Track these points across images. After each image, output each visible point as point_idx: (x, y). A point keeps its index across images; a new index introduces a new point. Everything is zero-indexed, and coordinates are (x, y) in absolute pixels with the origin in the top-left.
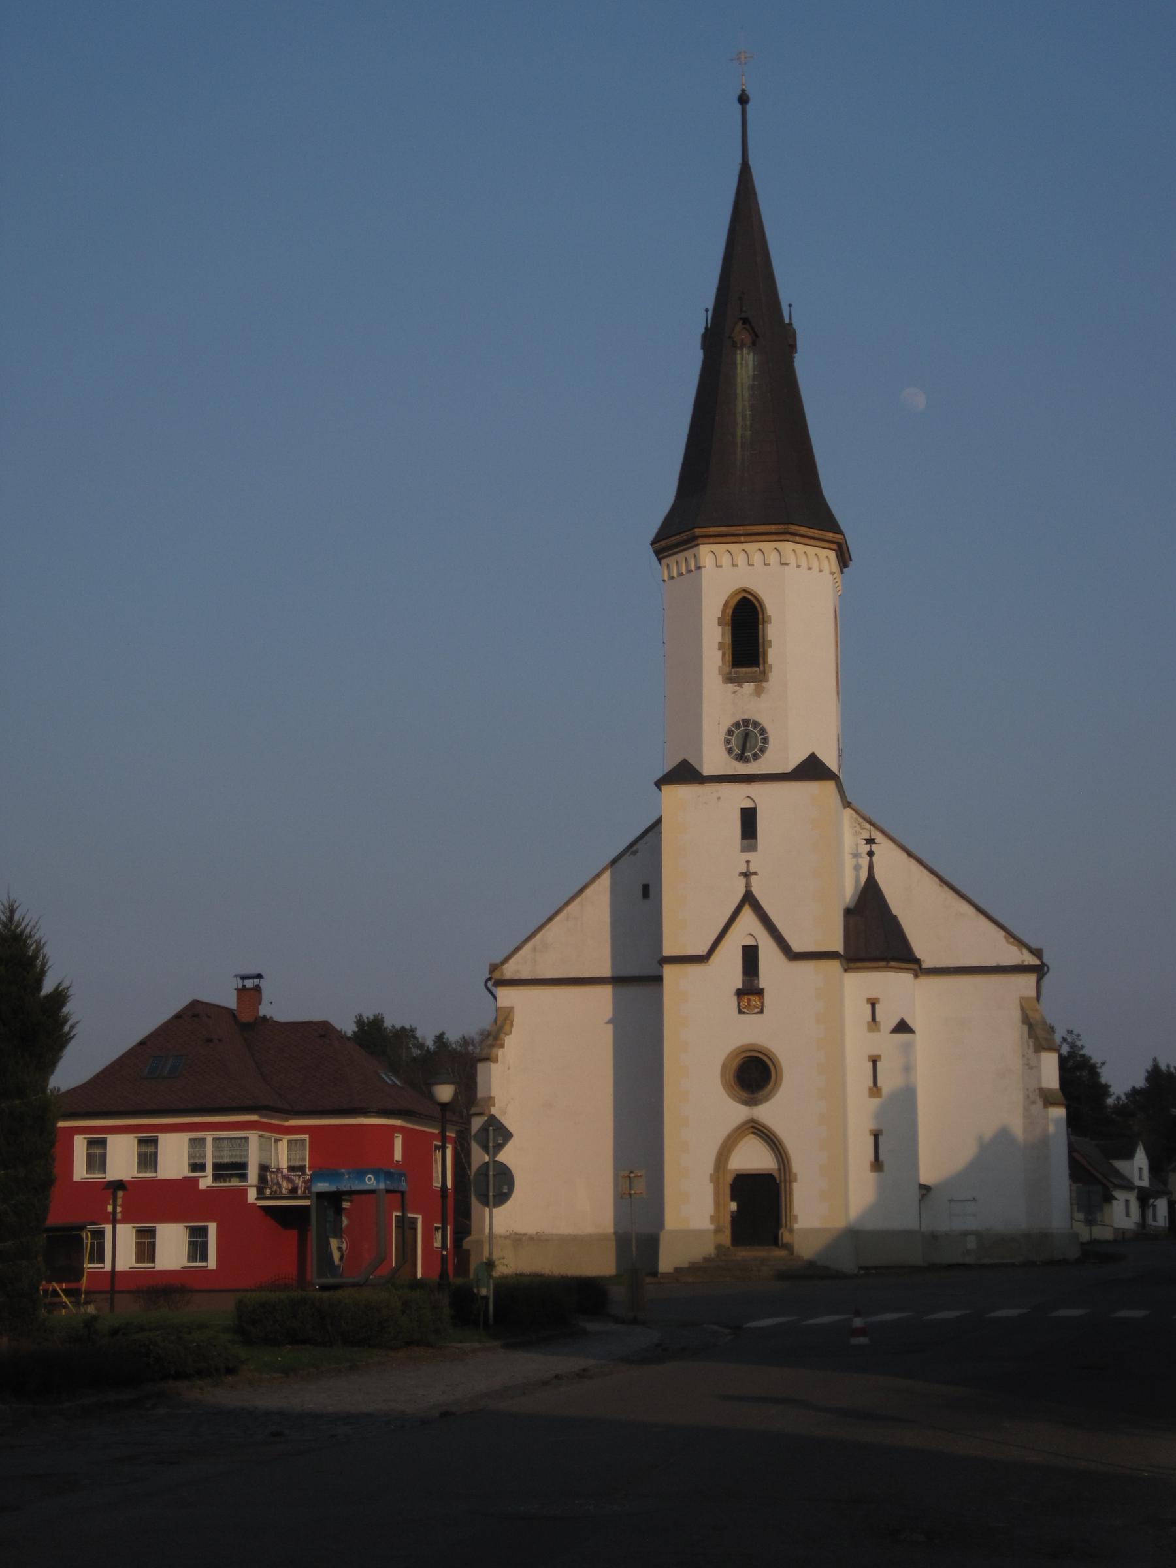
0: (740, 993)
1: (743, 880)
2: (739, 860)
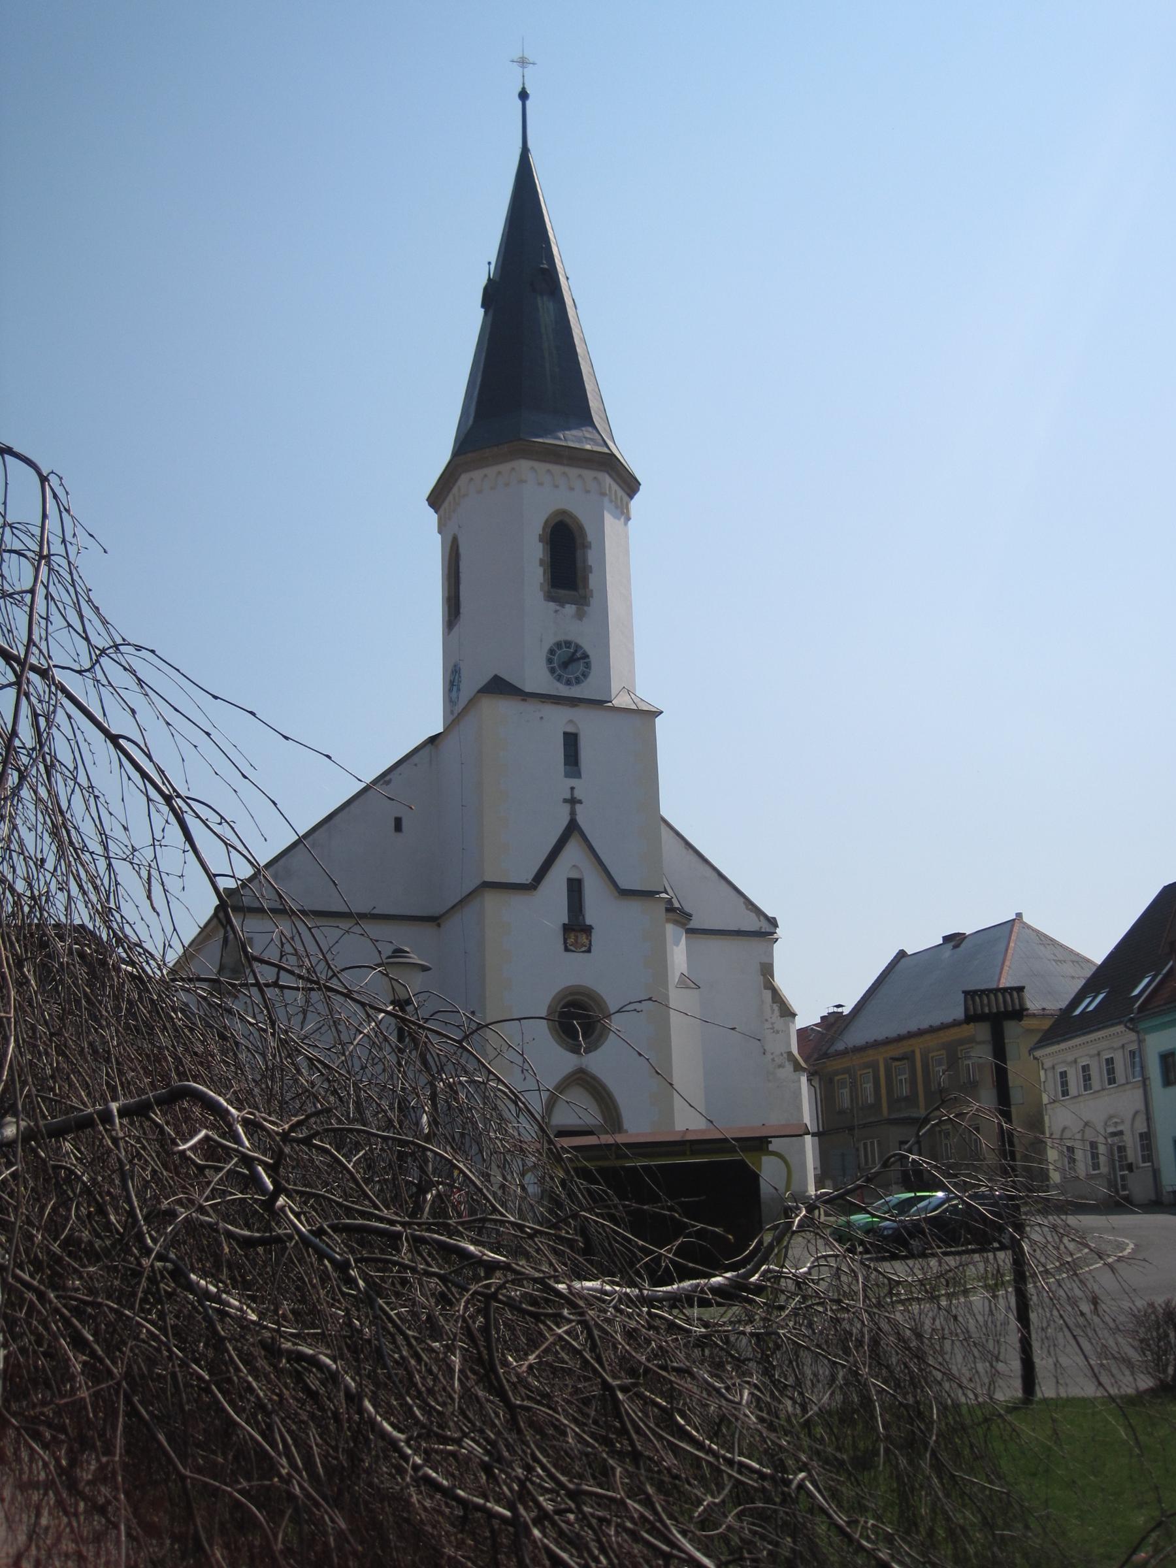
0: (567, 929)
1: (567, 807)
2: (563, 785)
